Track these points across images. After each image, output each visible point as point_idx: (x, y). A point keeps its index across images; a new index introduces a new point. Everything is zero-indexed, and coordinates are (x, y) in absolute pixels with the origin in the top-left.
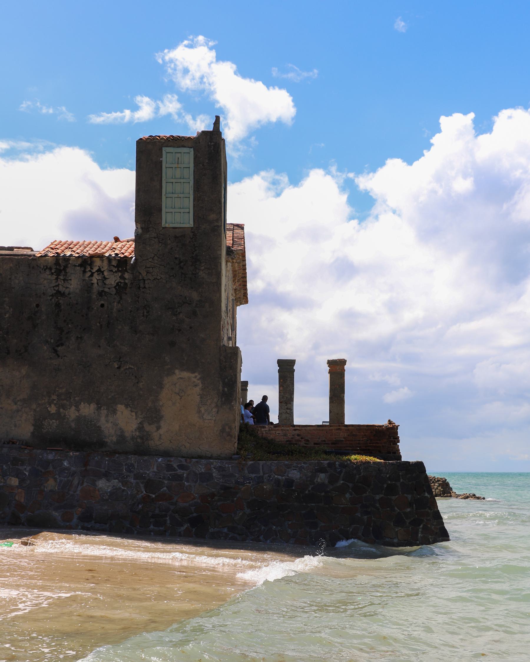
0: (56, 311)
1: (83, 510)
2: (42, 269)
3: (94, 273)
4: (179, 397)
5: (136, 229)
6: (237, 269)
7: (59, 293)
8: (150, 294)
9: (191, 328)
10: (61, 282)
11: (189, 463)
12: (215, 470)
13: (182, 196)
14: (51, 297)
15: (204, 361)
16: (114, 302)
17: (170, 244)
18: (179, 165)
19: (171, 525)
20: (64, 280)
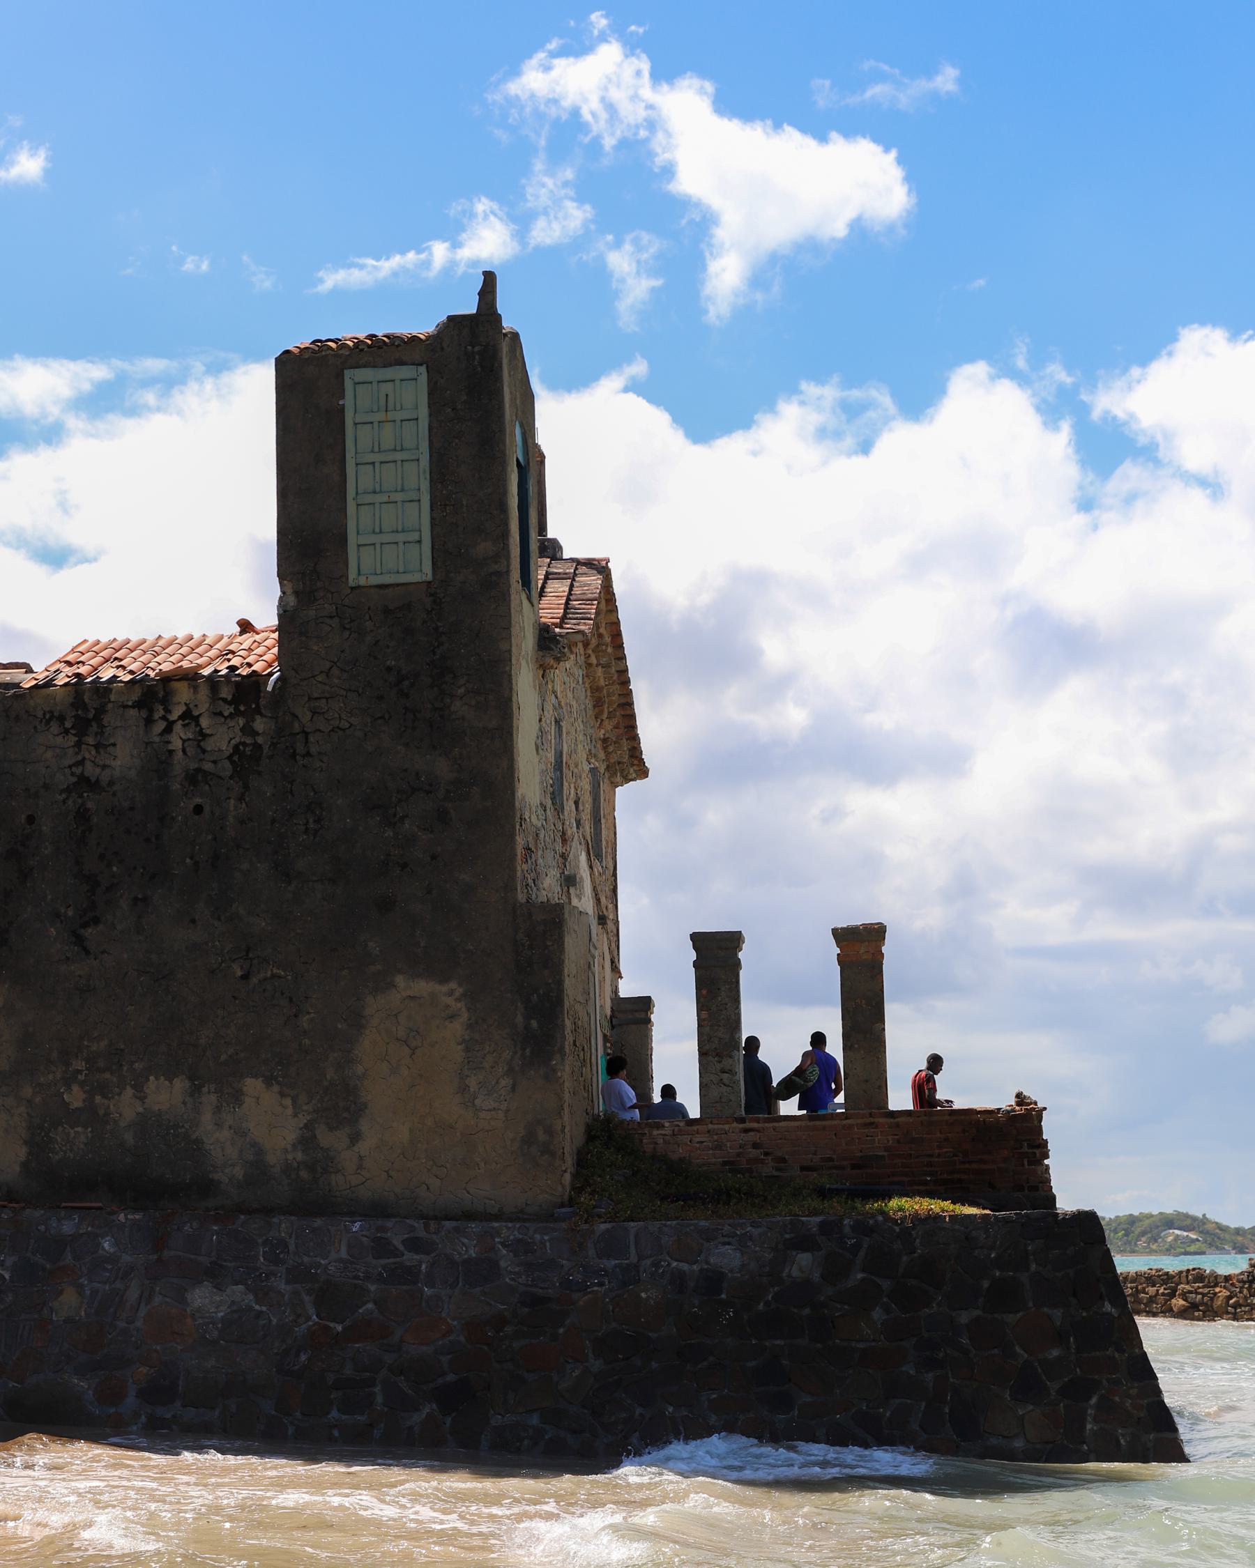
0: (80, 832)
1: (152, 1371)
2: (41, 722)
3: (174, 722)
4: (407, 1050)
5: (281, 597)
6: (602, 683)
7: (86, 784)
8: (322, 770)
9: (434, 857)
10: (88, 753)
11: (435, 1233)
12: (505, 1252)
13: (399, 497)
14: (64, 796)
15: (472, 947)
16: (229, 798)
17: (372, 631)
18: (391, 415)
19: (386, 1409)
20: (97, 747)
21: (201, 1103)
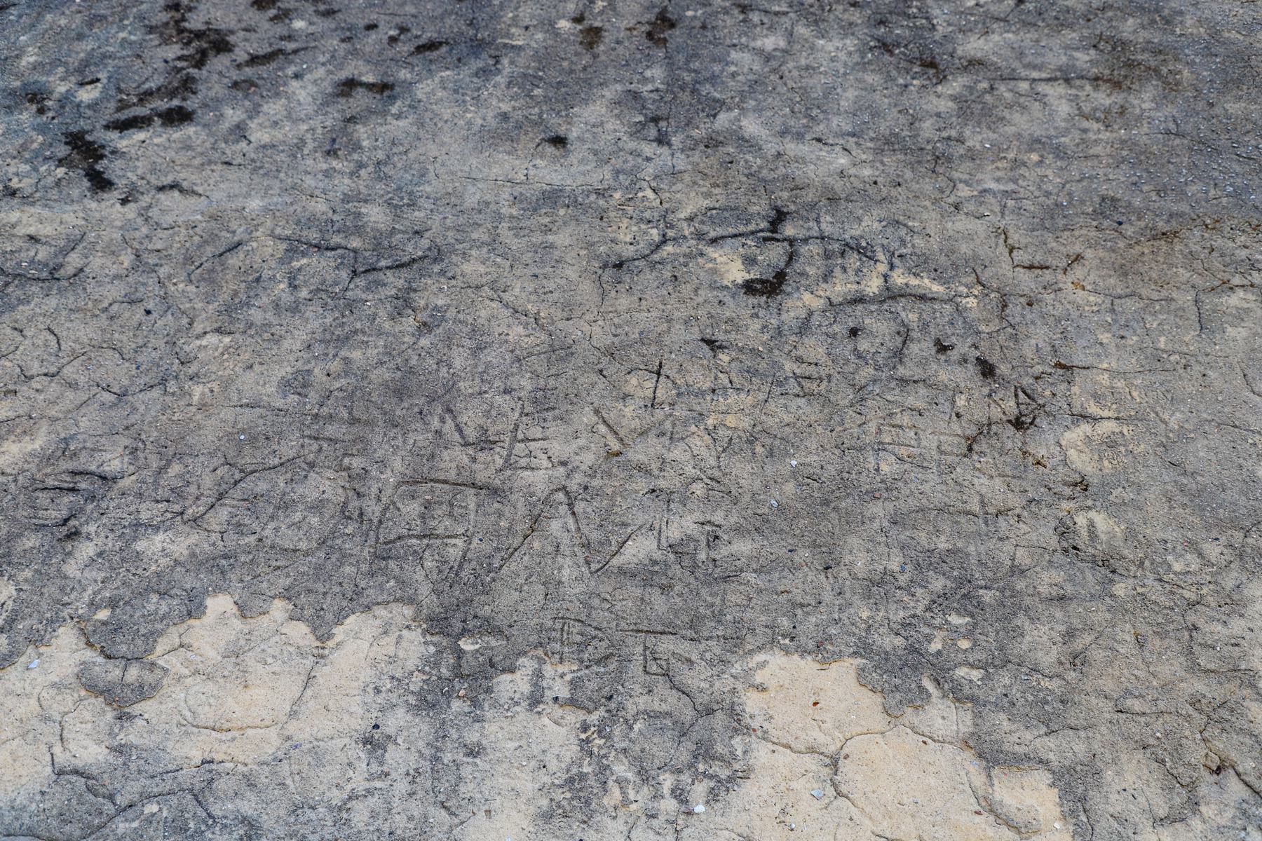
21: (474, 751)
